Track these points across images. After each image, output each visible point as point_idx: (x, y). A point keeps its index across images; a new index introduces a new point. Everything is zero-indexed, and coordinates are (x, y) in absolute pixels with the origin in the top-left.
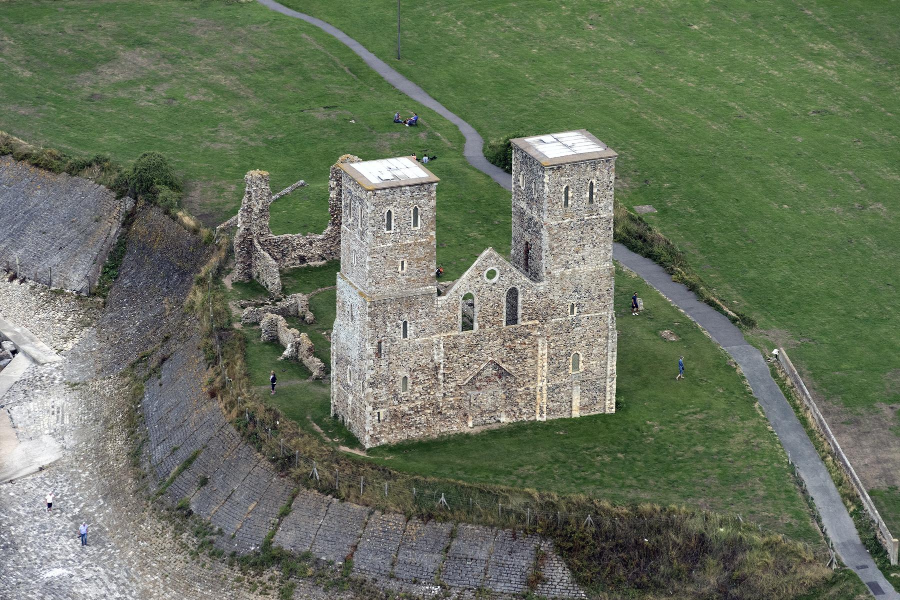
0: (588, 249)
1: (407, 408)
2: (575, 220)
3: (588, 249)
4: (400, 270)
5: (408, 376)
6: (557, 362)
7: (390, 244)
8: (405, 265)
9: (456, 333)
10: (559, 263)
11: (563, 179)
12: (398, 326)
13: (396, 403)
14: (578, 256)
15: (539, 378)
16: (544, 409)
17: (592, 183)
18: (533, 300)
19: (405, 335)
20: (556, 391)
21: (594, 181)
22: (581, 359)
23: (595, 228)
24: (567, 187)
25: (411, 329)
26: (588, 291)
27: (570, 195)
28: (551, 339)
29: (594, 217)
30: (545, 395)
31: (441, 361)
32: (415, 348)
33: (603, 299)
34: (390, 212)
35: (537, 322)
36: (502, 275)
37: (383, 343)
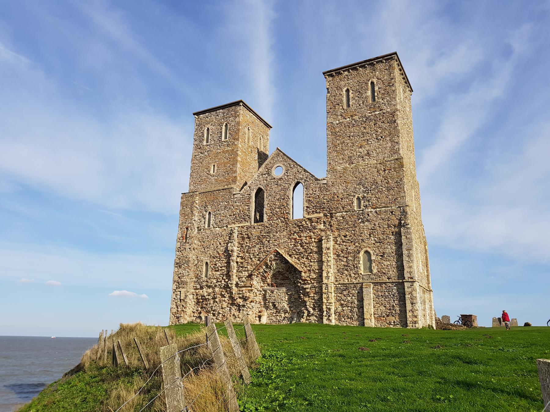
2: (356, 118)
3: (374, 143)
4: (212, 172)
5: (209, 262)
6: (345, 260)
7: (206, 154)
8: (216, 168)
9: (248, 224)
11: (343, 83)
14: (363, 151)
15: (324, 274)
17: (372, 83)
18: (318, 193)
19: (209, 226)
20: (345, 293)
21: (375, 80)
22: (373, 258)
24: (348, 91)
25: (212, 219)
27: (351, 95)
32: (216, 236)
35: (321, 215)
36: (287, 171)
37: (189, 229)
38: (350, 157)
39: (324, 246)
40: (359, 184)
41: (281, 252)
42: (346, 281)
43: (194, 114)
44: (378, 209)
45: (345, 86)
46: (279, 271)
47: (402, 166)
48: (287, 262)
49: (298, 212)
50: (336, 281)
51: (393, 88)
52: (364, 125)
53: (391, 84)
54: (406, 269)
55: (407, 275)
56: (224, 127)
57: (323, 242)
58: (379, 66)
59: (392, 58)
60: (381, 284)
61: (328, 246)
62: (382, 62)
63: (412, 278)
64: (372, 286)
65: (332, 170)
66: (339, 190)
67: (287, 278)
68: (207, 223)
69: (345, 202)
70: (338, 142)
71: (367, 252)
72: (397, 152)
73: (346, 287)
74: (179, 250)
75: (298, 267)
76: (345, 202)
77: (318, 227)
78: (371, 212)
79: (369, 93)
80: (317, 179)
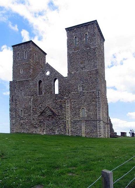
0: (86, 62)
1: (22, 122)
3: (86, 62)
4: (21, 73)
6: (75, 111)
8: (22, 71)
10: (74, 69)
12: (19, 91)
13: (19, 119)
14: (82, 66)
15: (67, 117)
16: (70, 131)
17: (86, 34)
20: (75, 124)
21: (87, 33)
23: (89, 53)
24: (76, 37)
26: (87, 80)
27: (77, 40)
28: (72, 101)
29: (88, 49)
30: (70, 125)
31: (31, 105)
33: (94, 84)
34: (18, 54)
38: (77, 68)
39: (67, 105)
40: (81, 80)
41: (50, 107)
42: (76, 120)
43: (12, 46)
44: (88, 91)
45: (75, 35)
46: (50, 115)
47: (97, 73)
48: (52, 111)
49: (57, 92)
50: (72, 120)
51: (95, 37)
52: (83, 54)
53: (94, 36)
54: (98, 116)
55: (98, 118)
56: (24, 53)
57: (66, 104)
58: (89, 27)
59: (94, 23)
60: (88, 121)
61: (68, 105)
62: (90, 24)
63: (100, 119)
64: (85, 122)
65: (69, 73)
66: (72, 82)
67: (53, 118)
68: (20, 94)
69: (75, 87)
70: (72, 61)
71: (83, 108)
72: (96, 67)
73: (75, 122)
74: (10, 104)
75: (57, 113)
76: (75, 87)
77: (64, 98)
78: (85, 92)
79: (85, 40)
80: (65, 77)
